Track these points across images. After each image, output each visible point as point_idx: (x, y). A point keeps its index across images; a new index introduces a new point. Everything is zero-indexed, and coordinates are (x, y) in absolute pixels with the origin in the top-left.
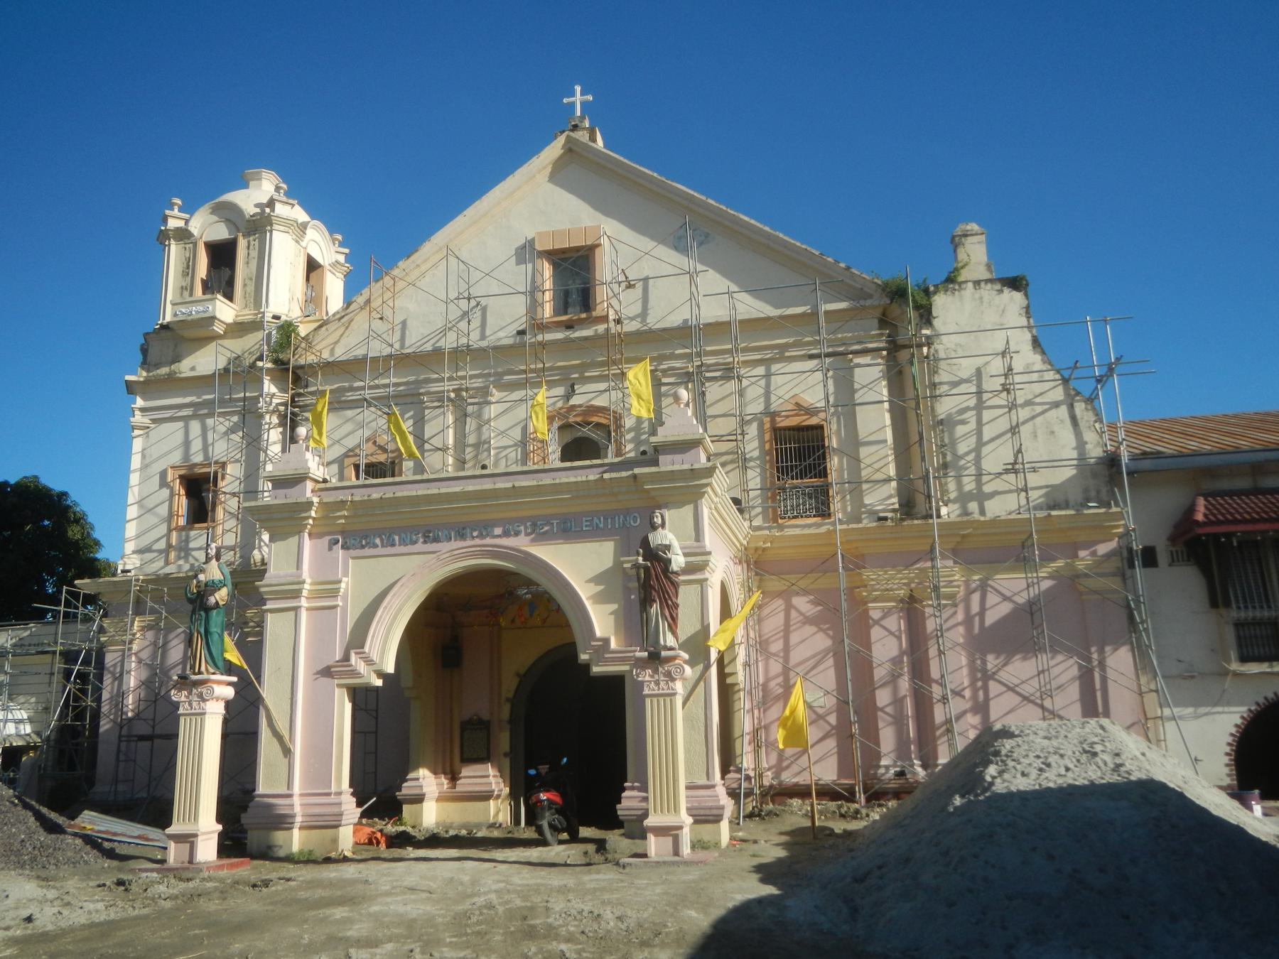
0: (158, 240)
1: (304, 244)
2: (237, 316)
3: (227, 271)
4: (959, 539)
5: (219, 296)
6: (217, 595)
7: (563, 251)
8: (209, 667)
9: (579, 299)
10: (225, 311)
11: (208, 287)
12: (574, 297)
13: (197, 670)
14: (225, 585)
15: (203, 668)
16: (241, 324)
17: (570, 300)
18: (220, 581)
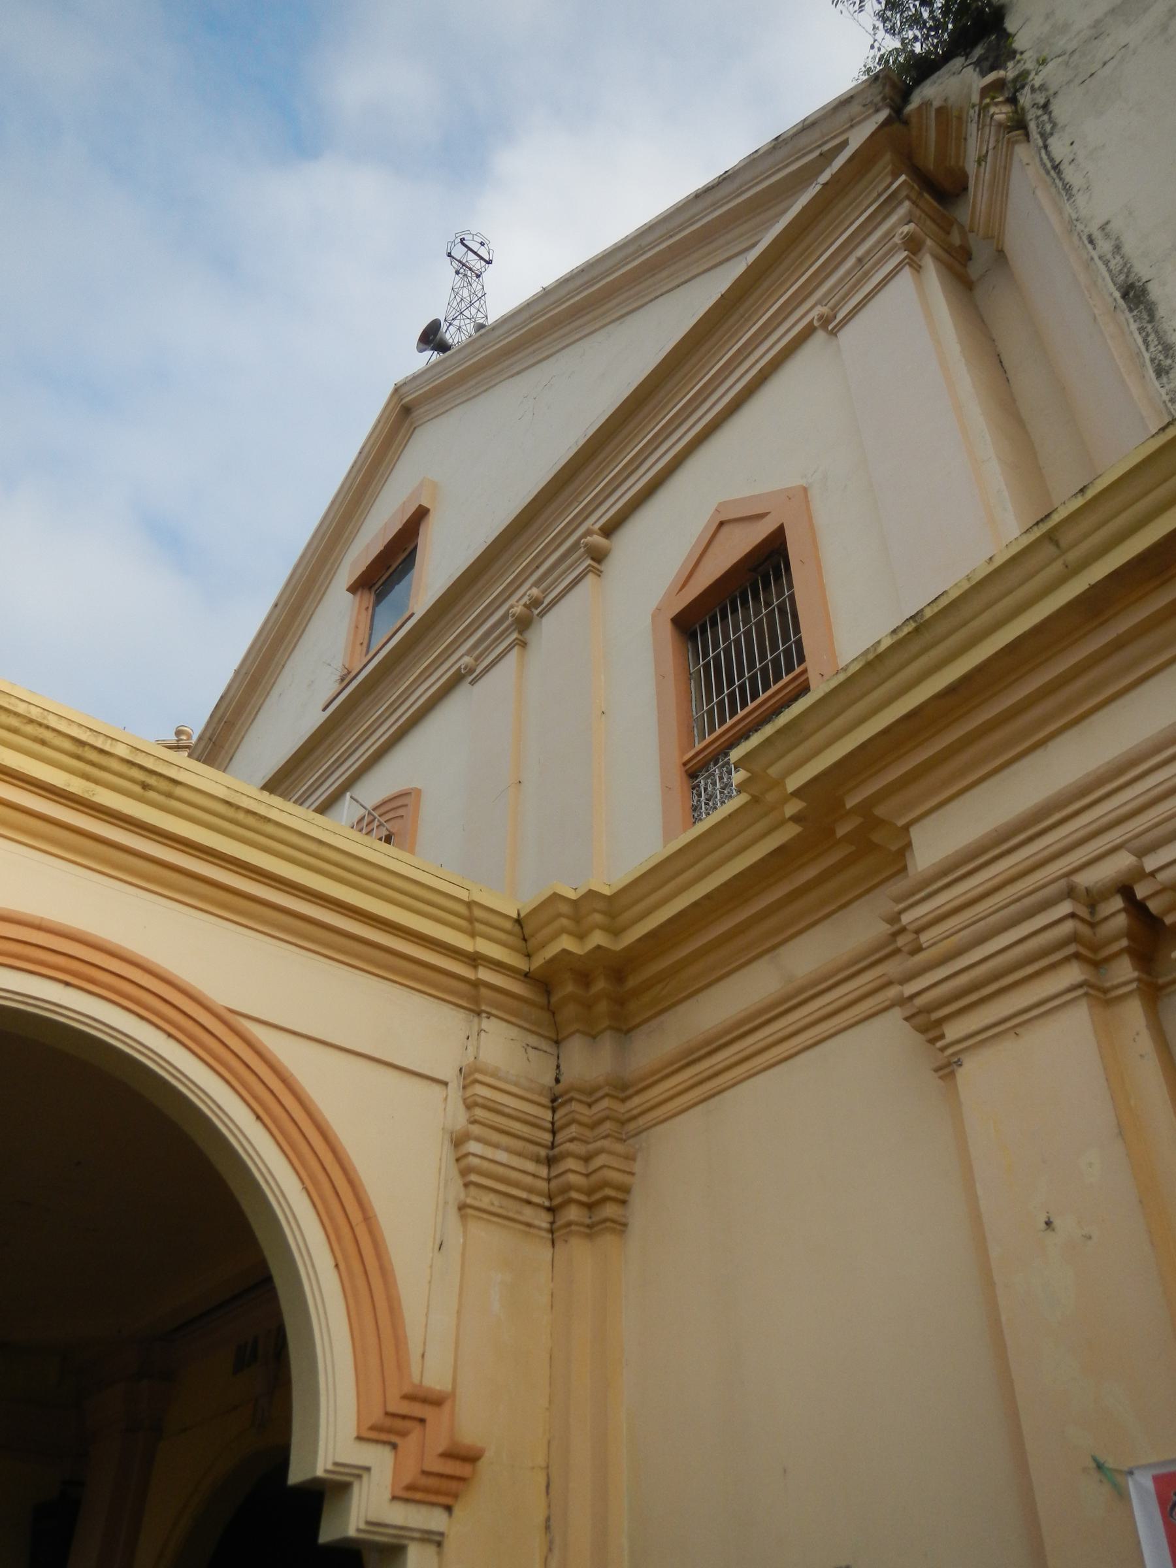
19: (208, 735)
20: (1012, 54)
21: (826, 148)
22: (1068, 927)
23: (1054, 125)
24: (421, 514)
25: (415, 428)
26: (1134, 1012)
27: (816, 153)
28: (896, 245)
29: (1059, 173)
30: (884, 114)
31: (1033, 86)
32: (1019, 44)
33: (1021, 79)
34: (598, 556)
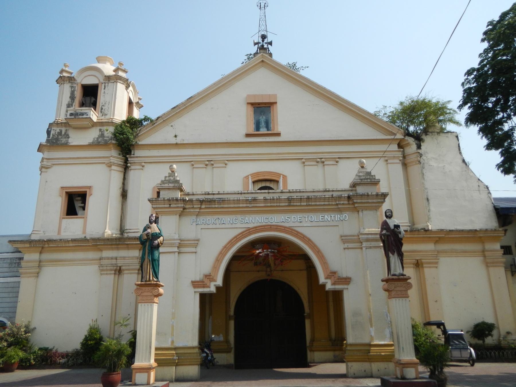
0: (56, 81)
1: (128, 91)
2: (97, 120)
3: (93, 99)
4: (438, 239)
5: (92, 109)
6: (159, 240)
7: (259, 104)
8: (154, 279)
9: (265, 125)
10: (94, 116)
11: (82, 104)
12: (263, 124)
13: (148, 279)
14: (162, 236)
15: (151, 279)
16: (102, 123)
17: (261, 126)
18: (159, 233)
19: (185, 104)
20: (421, 149)
21: (393, 131)
22: (414, 262)
23: (424, 168)
24: (276, 103)
25: (263, 67)
26: (415, 270)
27: (391, 130)
28: (399, 159)
29: (423, 175)
30: (403, 137)
31: (423, 158)
32: (422, 147)
33: (421, 154)
34: (337, 162)
